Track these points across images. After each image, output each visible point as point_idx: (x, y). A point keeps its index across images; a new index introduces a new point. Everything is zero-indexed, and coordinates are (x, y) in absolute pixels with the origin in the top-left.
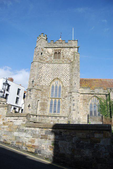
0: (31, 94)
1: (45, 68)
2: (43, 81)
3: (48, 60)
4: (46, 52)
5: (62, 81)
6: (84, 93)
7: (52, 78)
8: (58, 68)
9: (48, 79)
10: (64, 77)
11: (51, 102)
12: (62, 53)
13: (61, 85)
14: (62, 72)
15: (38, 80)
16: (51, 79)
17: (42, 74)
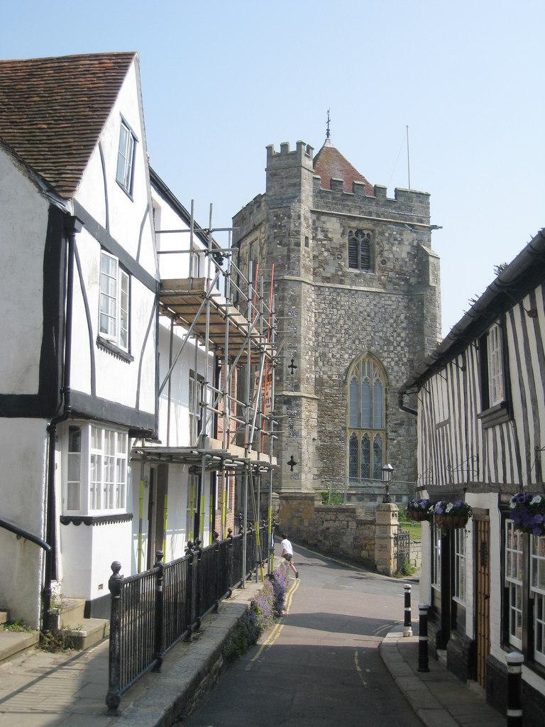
0: (292, 416)
1: (323, 306)
2: (321, 364)
3: (330, 270)
4: (320, 236)
5: (385, 364)
7: (350, 352)
8: (368, 310)
9: (338, 356)
10: (392, 348)
11: (354, 443)
12: (378, 244)
14: (385, 329)
15: (307, 357)
16: (346, 356)
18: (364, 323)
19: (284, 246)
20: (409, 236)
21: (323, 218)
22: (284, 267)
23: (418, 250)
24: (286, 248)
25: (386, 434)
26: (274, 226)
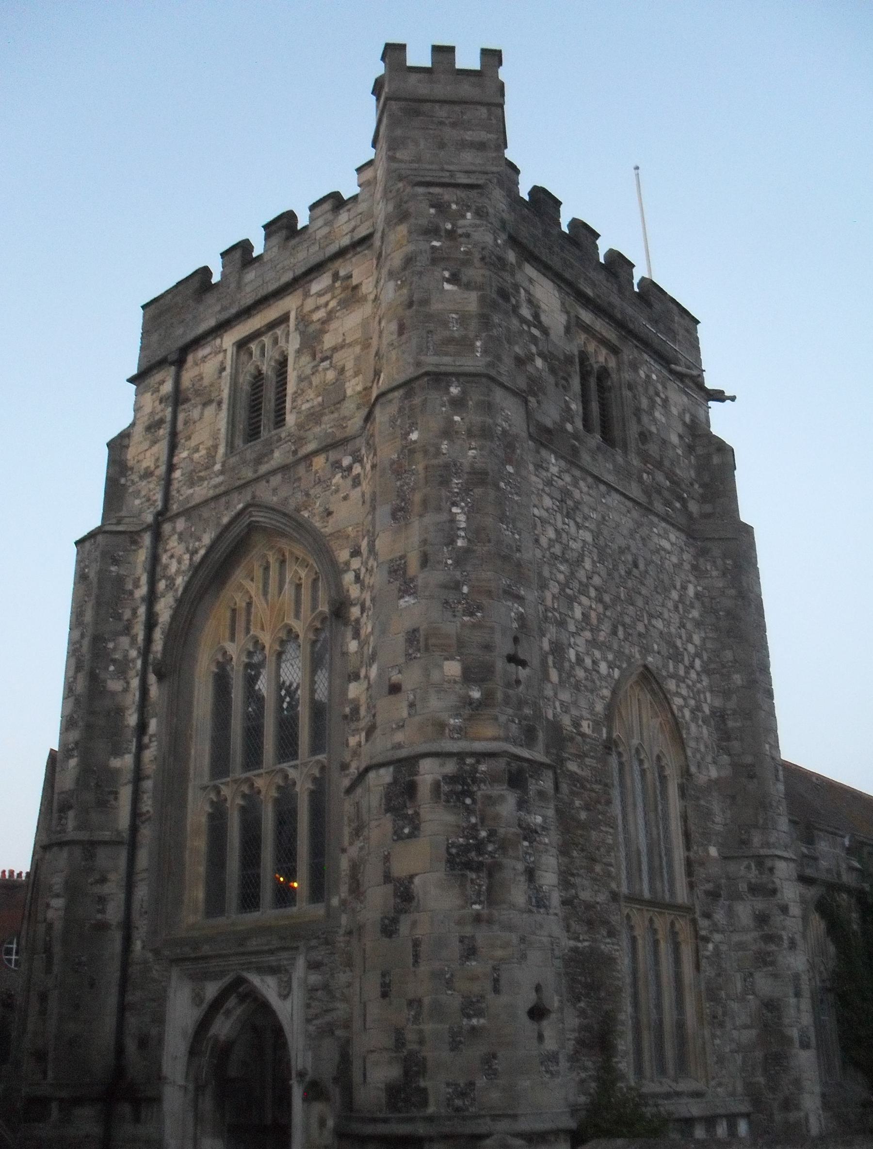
4: (526, 312)
9: (588, 662)
13: (672, 772)
18: (630, 584)
19: (468, 286)
20: (677, 399)
21: (530, 270)
22: (472, 345)
23: (694, 436)
24: (473, 296)
25: (694, 922)
26: (433, 231)
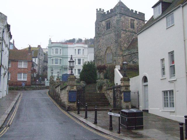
4: (102, 26)
6: (125, 54)
15: (98, 52)
17: (101, 46)
